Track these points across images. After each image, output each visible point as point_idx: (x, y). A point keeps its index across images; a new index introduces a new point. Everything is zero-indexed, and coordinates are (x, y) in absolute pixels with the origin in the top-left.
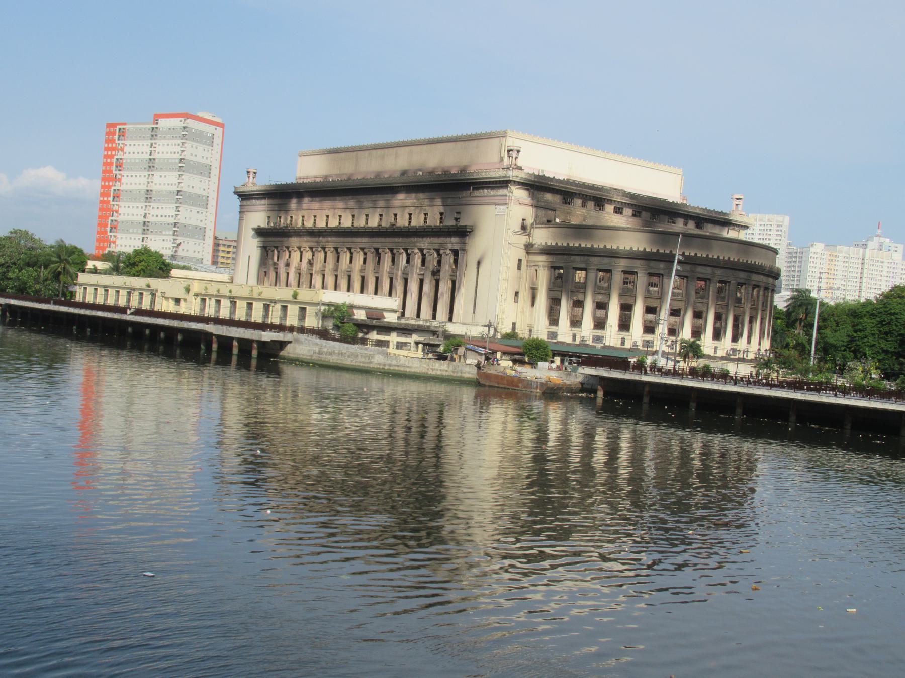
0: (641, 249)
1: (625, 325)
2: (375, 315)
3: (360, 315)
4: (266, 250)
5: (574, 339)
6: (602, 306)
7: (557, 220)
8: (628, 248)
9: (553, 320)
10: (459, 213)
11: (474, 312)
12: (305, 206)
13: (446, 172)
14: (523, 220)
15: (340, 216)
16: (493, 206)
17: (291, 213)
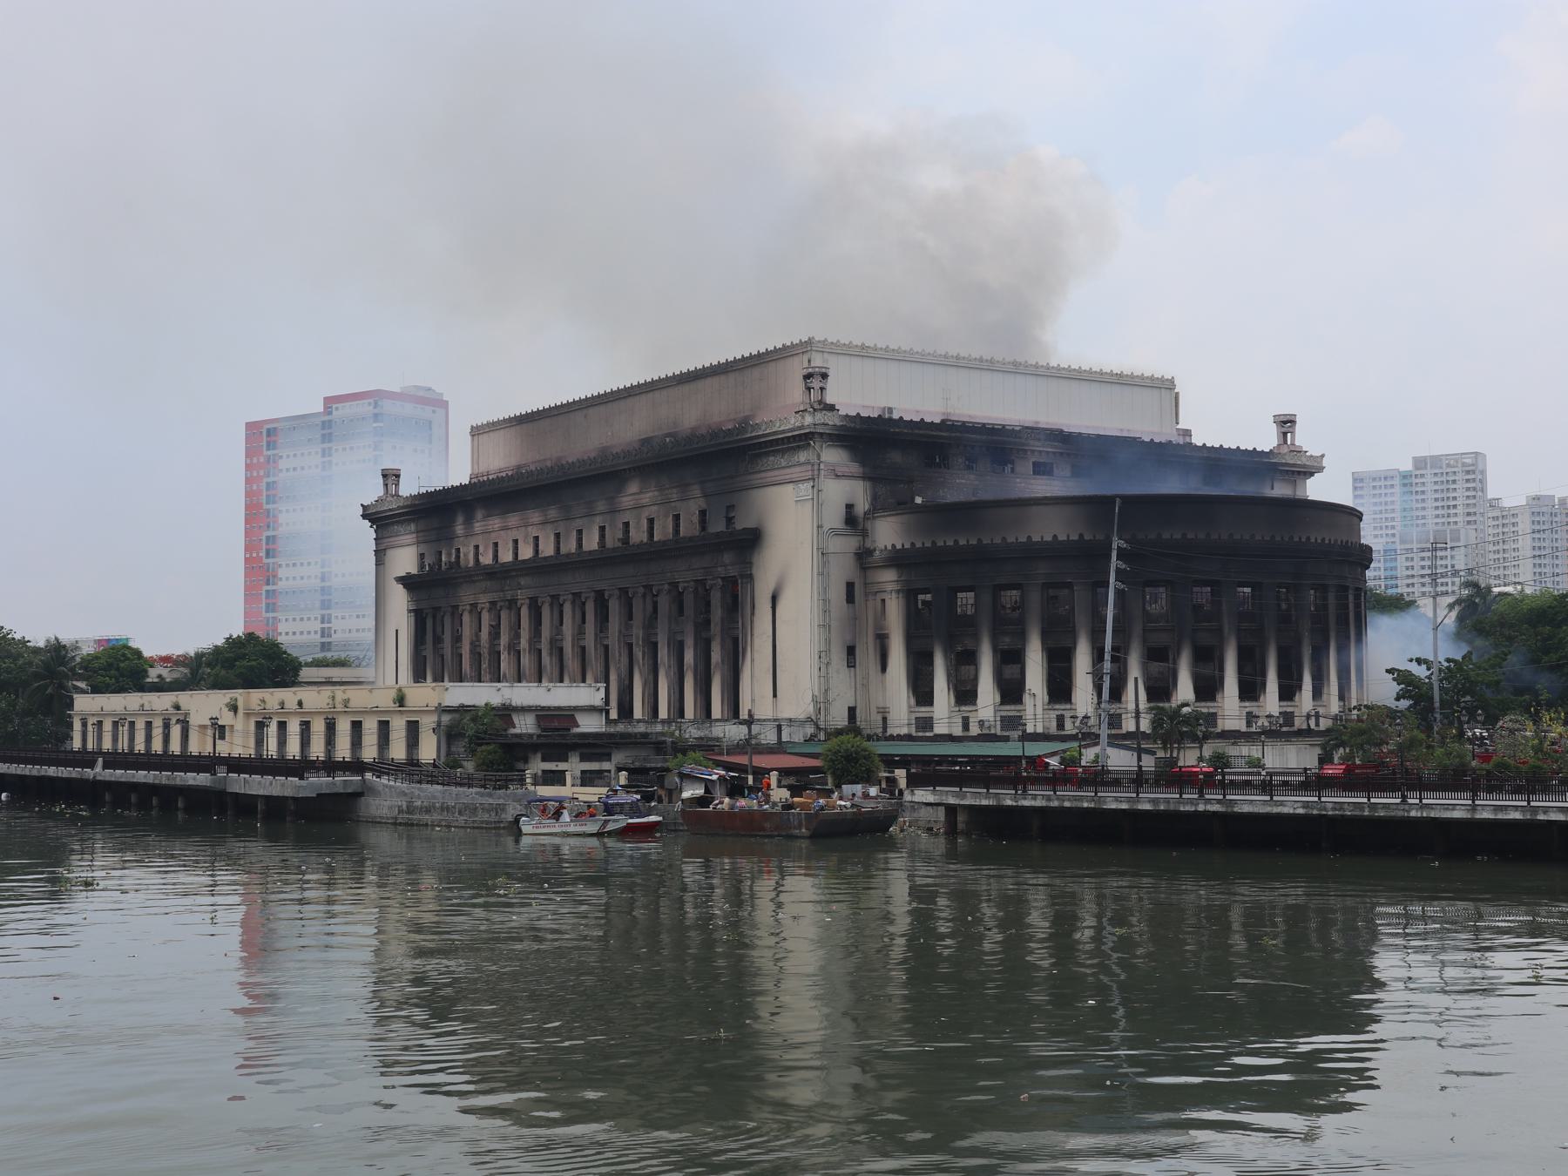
0: (1075, 537)
1: (1060, 689)
2: (556, 723)
3: (525, 725)
4: (423, 622)
5: (966, 726)
6: (1010, 660)
7: (919, 500)
8: (1048, 538)
9: (922, 692)
10: (731, 508)
11: (775, 695)
12: (478, 527)
13: (715, 433)
14: (849, 507)
15: (537, 538)
16: (791, 486)
17: (458, 543)
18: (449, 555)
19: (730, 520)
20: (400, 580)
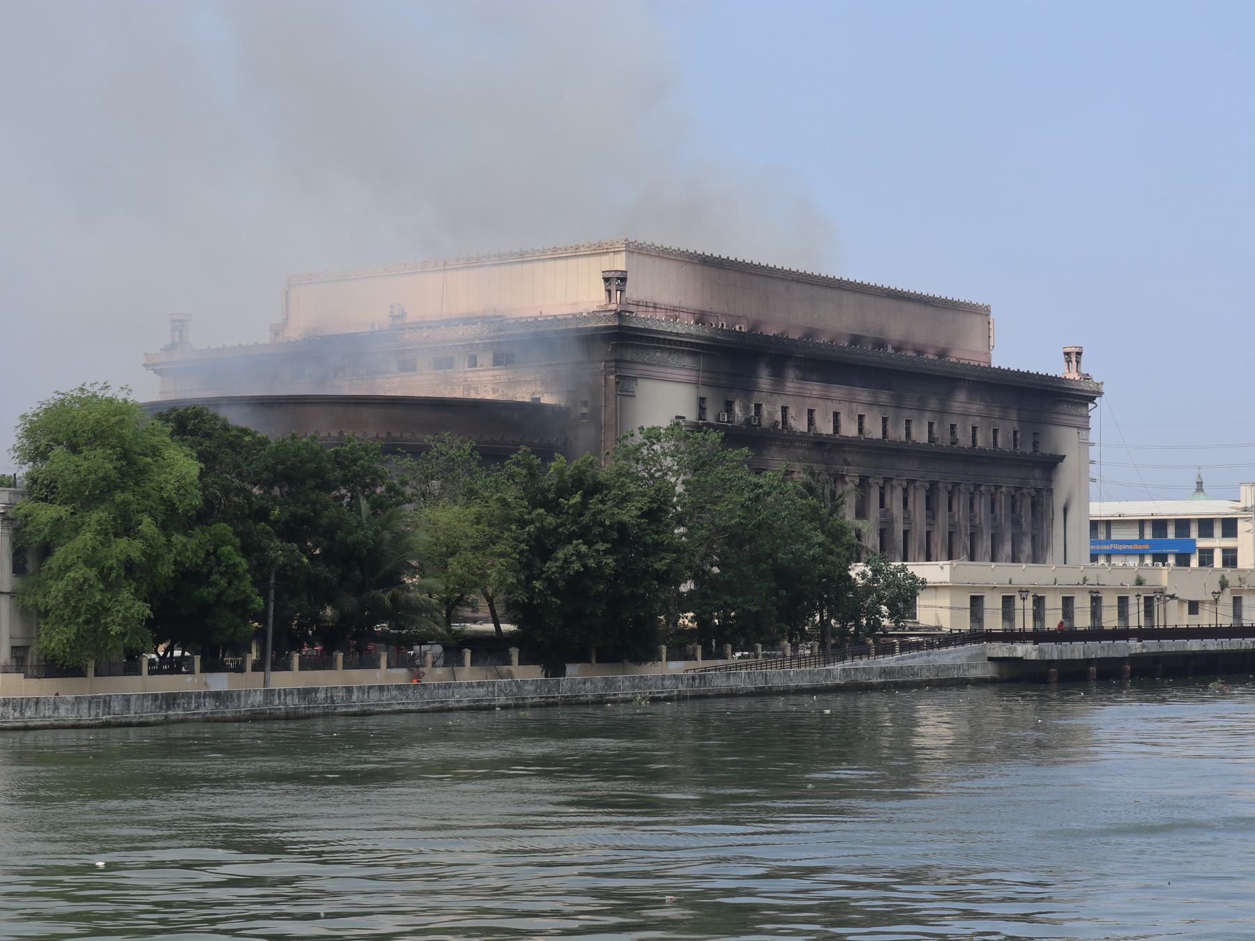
10: (1036, 434)
12: (791, 386)
16: (1075, 430)
17: (756, 398)
18: (746, 409)
19: (1035, 444)
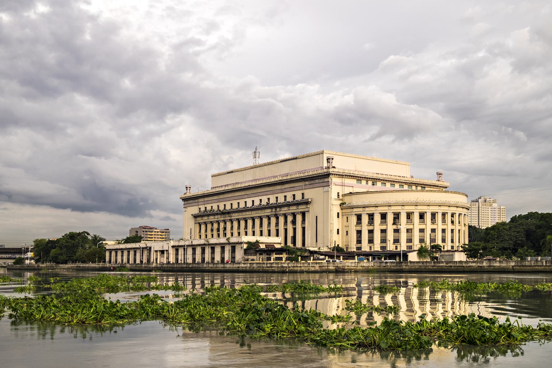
3: (262, 246)
20: (192, 215)
